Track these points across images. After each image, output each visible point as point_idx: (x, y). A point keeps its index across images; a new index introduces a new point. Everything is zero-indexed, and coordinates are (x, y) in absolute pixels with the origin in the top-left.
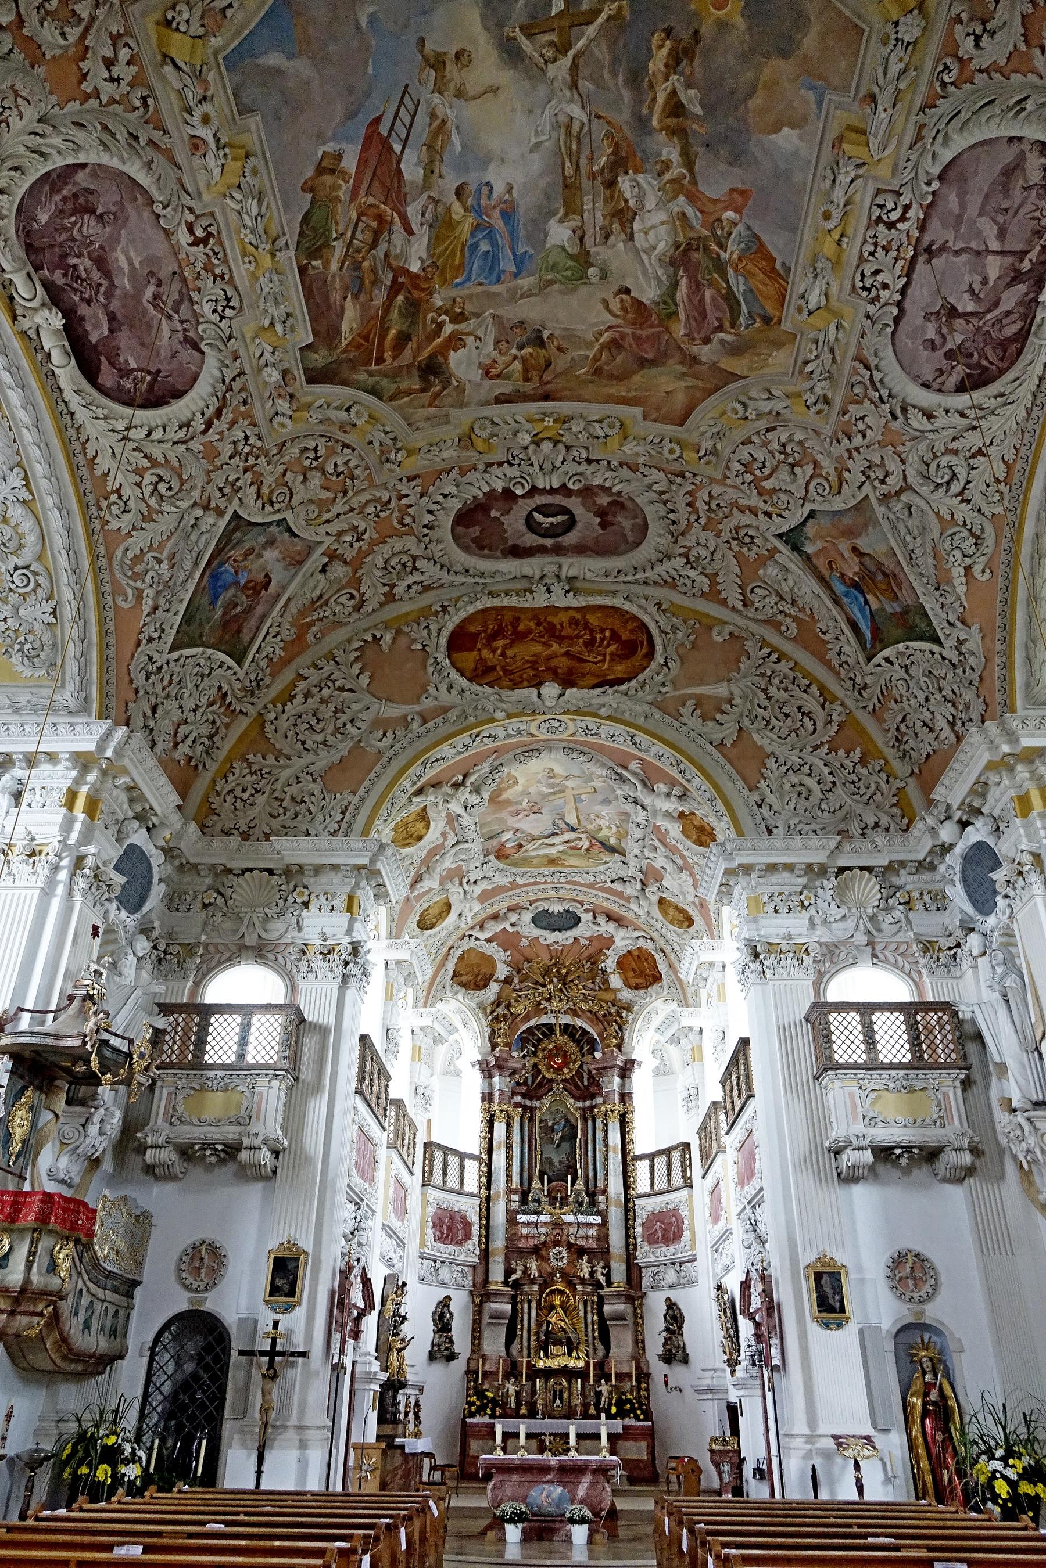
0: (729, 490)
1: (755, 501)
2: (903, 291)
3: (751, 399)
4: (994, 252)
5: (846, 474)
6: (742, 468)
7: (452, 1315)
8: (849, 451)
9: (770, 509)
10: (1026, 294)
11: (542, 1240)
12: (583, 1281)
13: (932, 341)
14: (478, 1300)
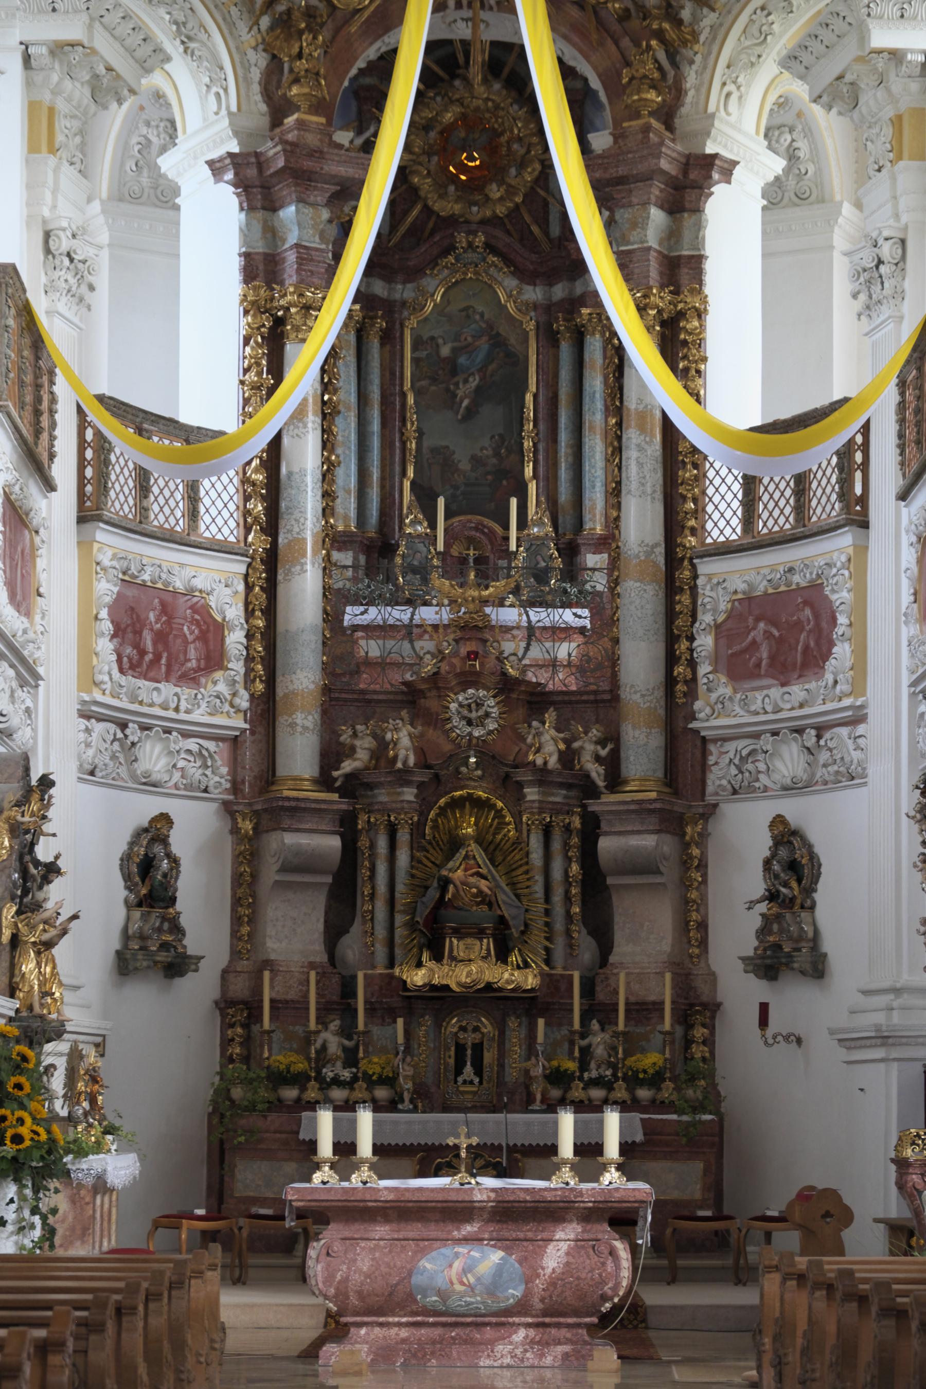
7: (175, 862)
11: (428, 668)
12: (543, 776)
14: (247, 826)
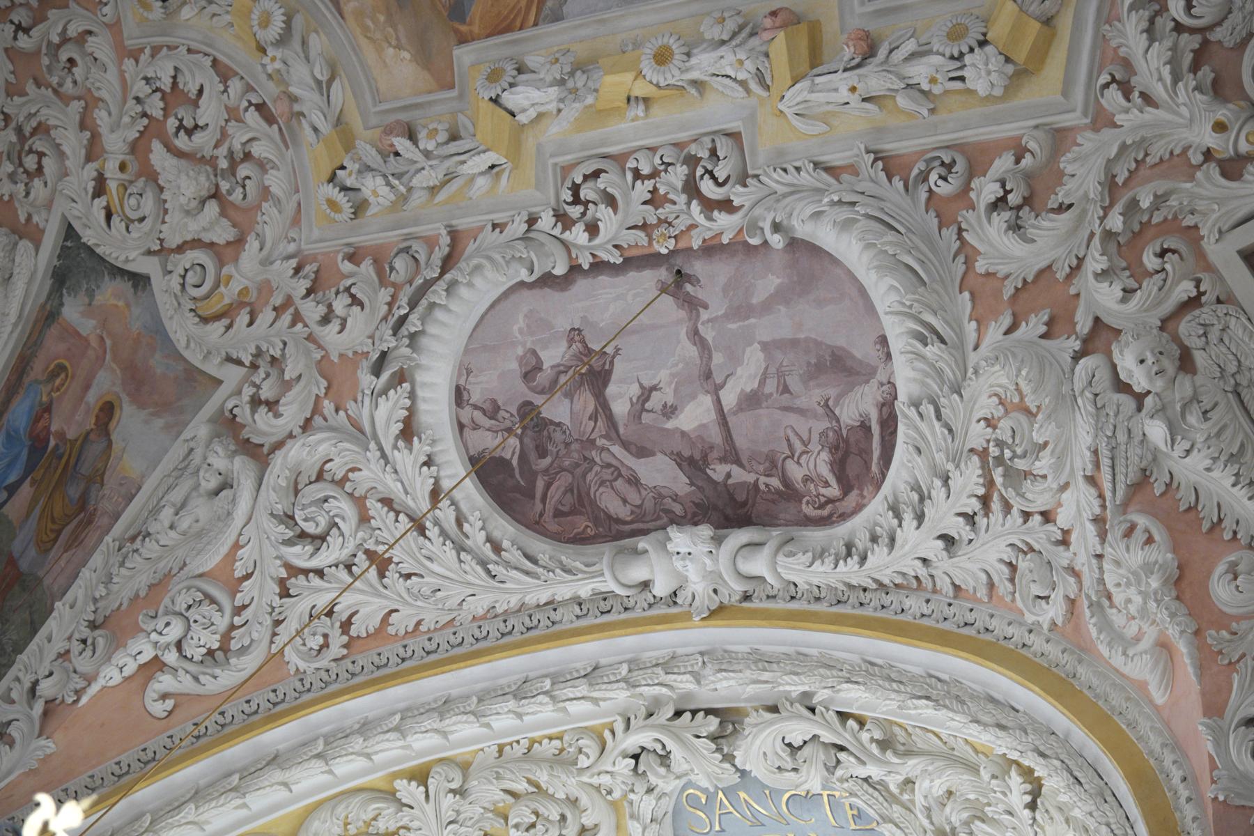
0: (112, 75)
1: (116, 143)
2: (599, 266)
3: (304, 43)
4: (718, 402)
5: (243, 318)
6: (166, 84)
8: (288, 302)
9: (112, 186)
10: (675, 498)
13: (538, 368)
